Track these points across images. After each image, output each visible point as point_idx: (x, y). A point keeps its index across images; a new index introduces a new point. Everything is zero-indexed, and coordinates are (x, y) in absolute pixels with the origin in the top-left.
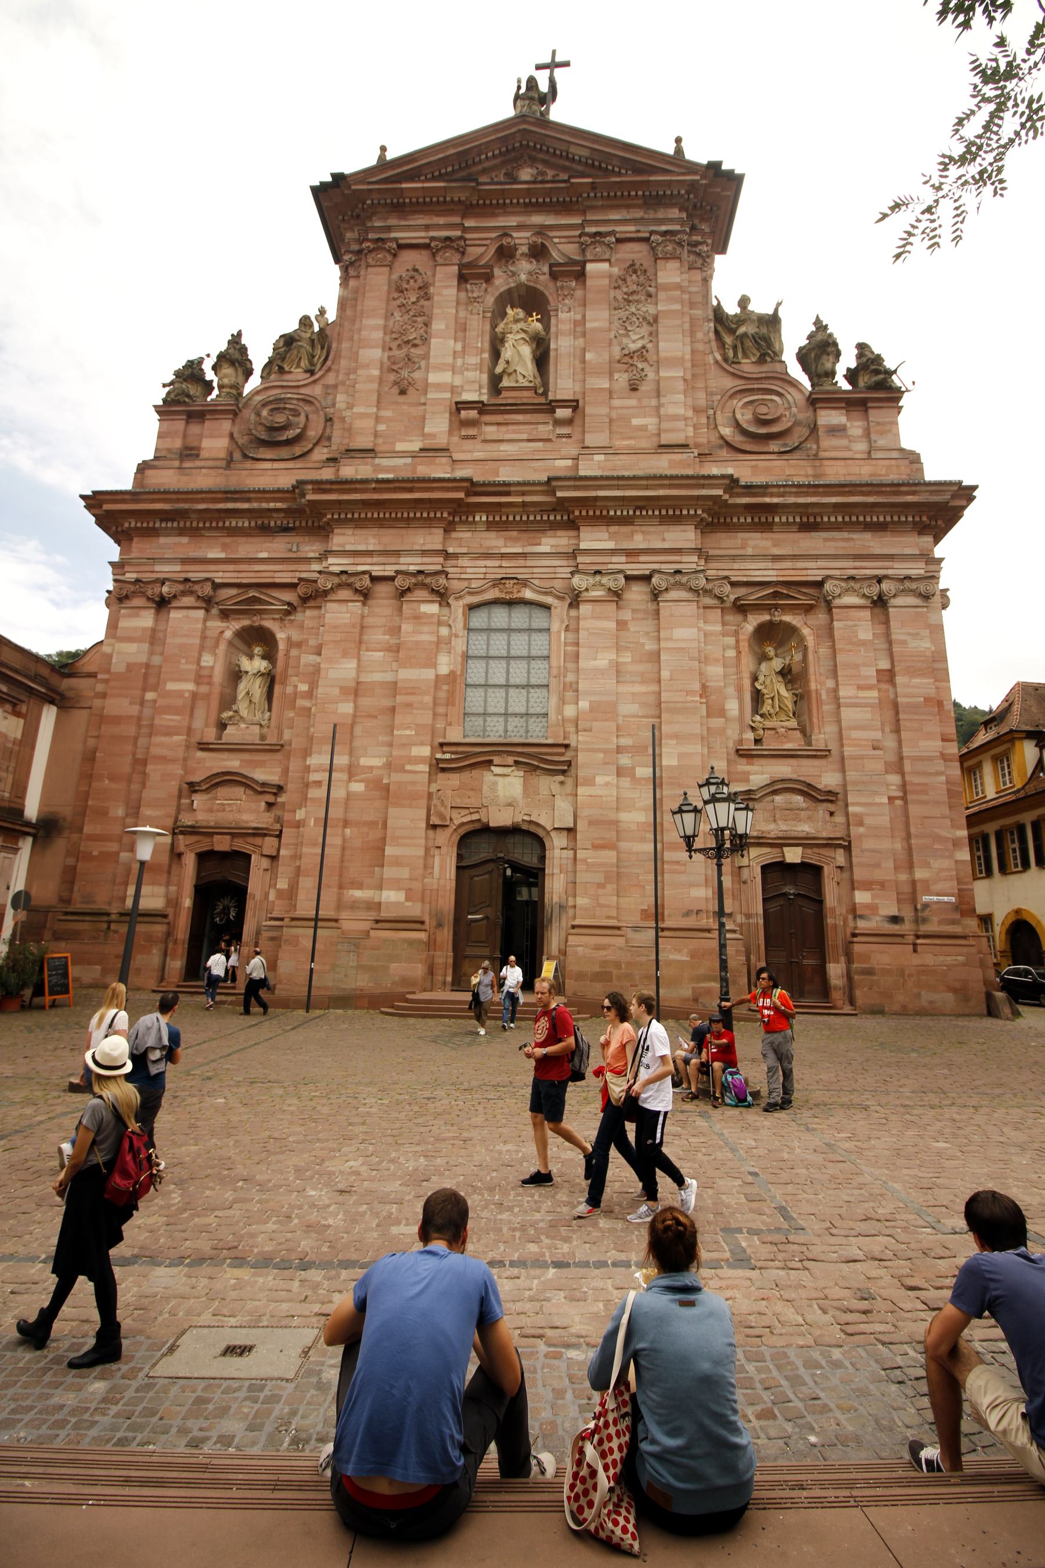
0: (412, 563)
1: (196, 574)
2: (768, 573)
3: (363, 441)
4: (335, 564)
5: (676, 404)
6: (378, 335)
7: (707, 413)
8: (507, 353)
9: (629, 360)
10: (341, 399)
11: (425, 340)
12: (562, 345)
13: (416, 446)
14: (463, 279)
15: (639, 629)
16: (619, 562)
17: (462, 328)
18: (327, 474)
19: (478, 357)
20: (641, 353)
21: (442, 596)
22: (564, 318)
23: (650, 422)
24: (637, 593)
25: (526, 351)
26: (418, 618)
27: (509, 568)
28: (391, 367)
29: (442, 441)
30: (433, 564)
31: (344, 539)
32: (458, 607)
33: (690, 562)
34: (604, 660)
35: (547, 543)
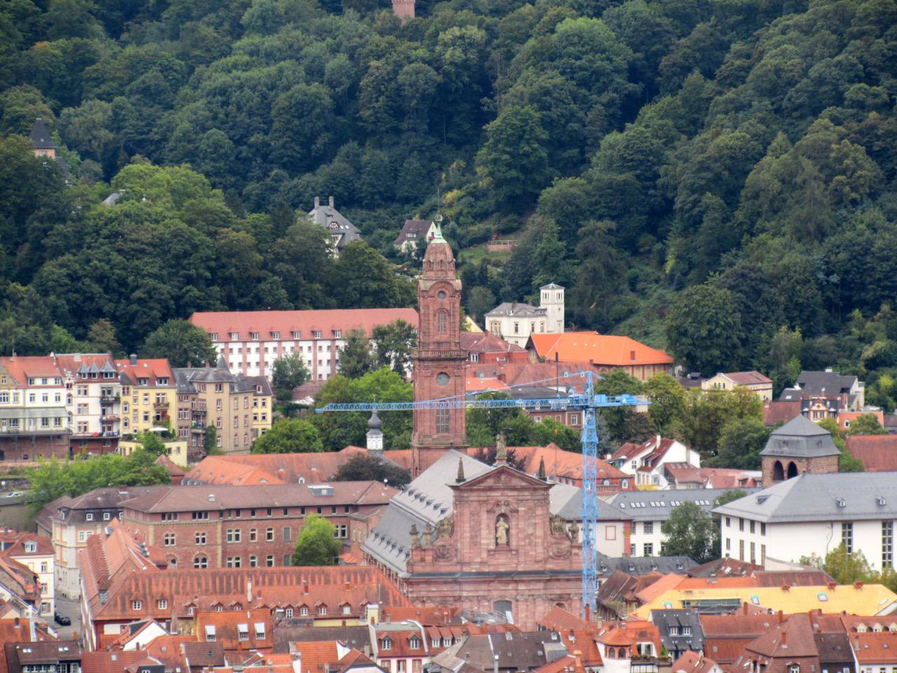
0: (481, 593)
1: (431, 595)
2: (558, 592)
3: (467, 560)
4: (464, 594)
5: (540, 549)
6: (468, 529)
7: (546, 549)
8: (499, 534)
9: (529, 536)
10: (459, 545)
11: (480, 529)
12: (513, 532)
13: (478, 560)
14: (489, 512)
15: (531, 607)
16: (527, 593)
17: (488, 526)
18: (458, 568)
19: (492, 536)
20: (532, 535)
21: (489, 601)
22: (513, 523)
23: (532, 553)
24: (531, 598)
25: (504, 532)
26: (484, 606)
27: (503, 593)
28: (472, 538)
29: (485, 560)
30: (486, 594)
31: (466, 587)
32: (492, 602)
33: (542, 592)
34: (523, 615)
35: (510, 587)
